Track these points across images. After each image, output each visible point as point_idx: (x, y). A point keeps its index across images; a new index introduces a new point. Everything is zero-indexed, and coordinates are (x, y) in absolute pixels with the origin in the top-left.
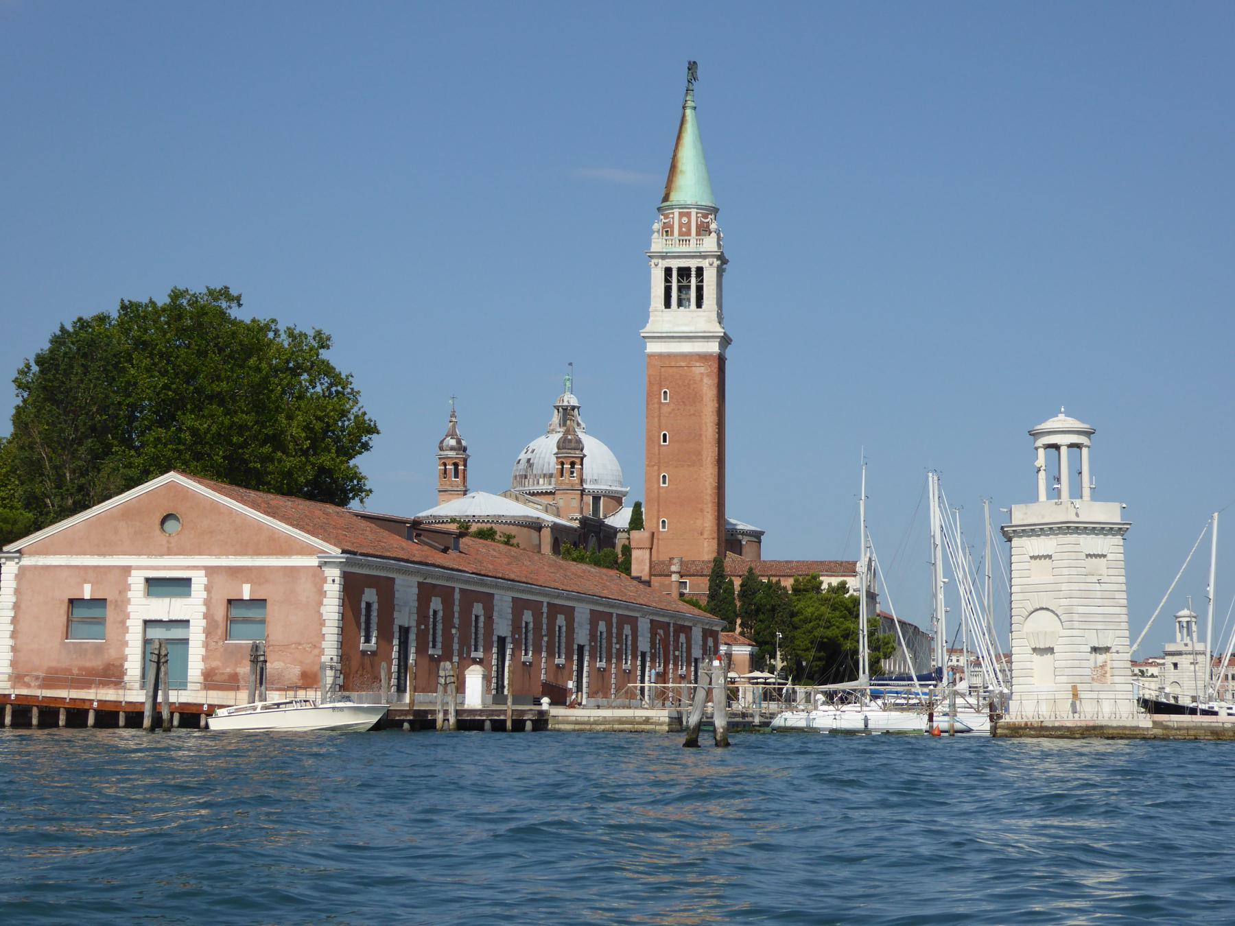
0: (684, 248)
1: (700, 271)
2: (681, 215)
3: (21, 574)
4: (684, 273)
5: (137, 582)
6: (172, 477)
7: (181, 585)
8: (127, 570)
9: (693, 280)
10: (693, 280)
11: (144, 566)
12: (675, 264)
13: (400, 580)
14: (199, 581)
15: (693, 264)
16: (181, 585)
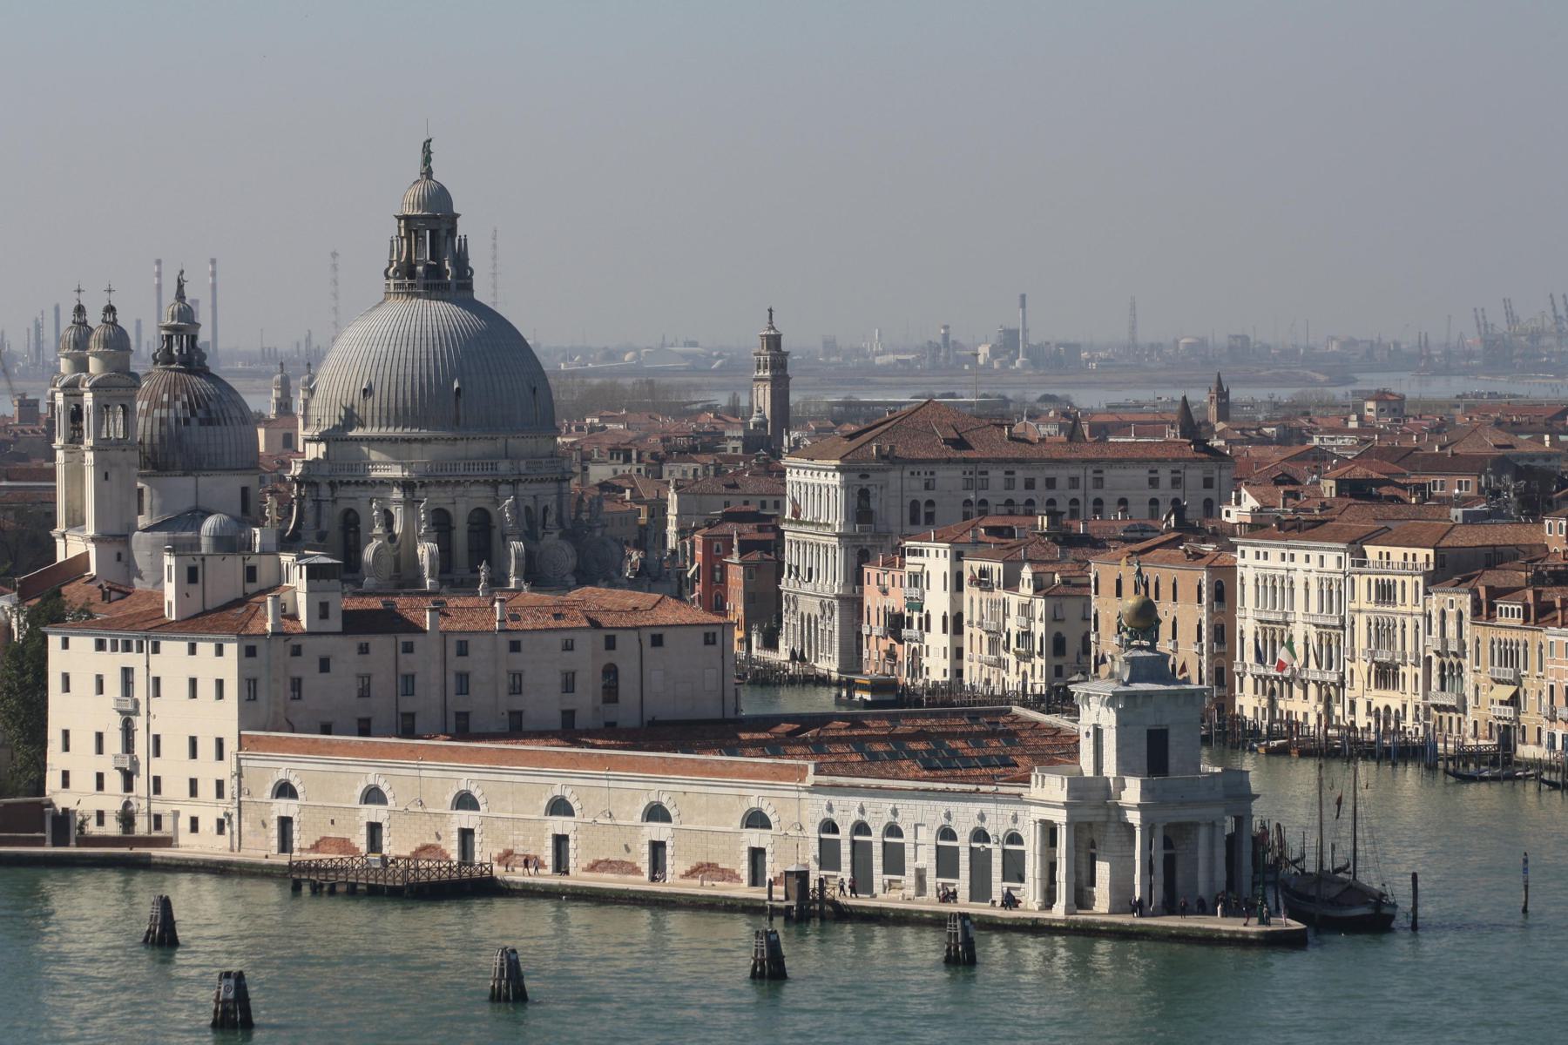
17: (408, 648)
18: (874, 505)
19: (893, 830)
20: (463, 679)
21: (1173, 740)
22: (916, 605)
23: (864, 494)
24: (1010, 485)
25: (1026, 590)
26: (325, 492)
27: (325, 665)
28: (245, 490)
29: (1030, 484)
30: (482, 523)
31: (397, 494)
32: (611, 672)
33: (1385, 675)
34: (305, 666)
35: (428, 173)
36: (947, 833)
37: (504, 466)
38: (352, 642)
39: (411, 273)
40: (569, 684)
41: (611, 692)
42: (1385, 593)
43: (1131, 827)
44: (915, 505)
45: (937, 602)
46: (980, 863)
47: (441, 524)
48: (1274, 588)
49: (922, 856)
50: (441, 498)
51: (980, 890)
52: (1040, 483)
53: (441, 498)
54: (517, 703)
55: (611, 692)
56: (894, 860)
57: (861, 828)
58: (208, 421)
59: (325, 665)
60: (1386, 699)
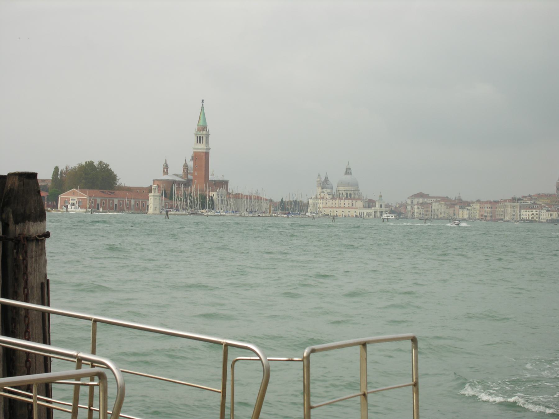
0: (200, 133)
1: (203, 137)
2: (200, 127)
3: (61, 198)
4: (200, 137)
5: (71, 199)
6: (74, 189)
7: (75, 199)
8: (70, 198)
9: (202, 139)
10: (202, 139)
11: (71, 197)
12: (199, 136)
13: (97, 199)
14: (76, 199)
15: (202, 136)
16: (75, 199)
17: (336, 201)
18: (413, 202)
19: (364, 212)
20: (340, 203)
21: (382, 205)
22: (414, 211)
23: (412, 201)
24: (427, 200)
25: (421, 208)
26: (338, 191)
27: (329, 202)
28: (331, 191)
29: (429, 200)
30: (350, 194)
31: (344, 191)
32: (353, 204)
33: (441, 213)
34: (327, 202)
35: (348, 164)
36: (367, 212)
37: (353, 190)
38: (331, 200)
39: (346, 173)
40: (349, 204)
41: (353, 205)
42: (441, 206)
43: (378, 211)
44: (417, 202)
45: (416, 211)
46: (369, 214)
47: (347, 194)
48: (435, 206)
49: (365, 214)
50: (347, 192)
51: (369, 216)
52: (430, 200)
53: (347, 192)
54: (345, 205)
55: (353, 205)
56: (364, 214)
57: (362, 212)
58: (328, 185)
59: (329, 202)
60: (441, 216)
